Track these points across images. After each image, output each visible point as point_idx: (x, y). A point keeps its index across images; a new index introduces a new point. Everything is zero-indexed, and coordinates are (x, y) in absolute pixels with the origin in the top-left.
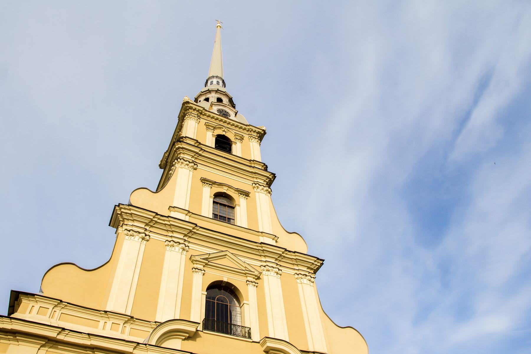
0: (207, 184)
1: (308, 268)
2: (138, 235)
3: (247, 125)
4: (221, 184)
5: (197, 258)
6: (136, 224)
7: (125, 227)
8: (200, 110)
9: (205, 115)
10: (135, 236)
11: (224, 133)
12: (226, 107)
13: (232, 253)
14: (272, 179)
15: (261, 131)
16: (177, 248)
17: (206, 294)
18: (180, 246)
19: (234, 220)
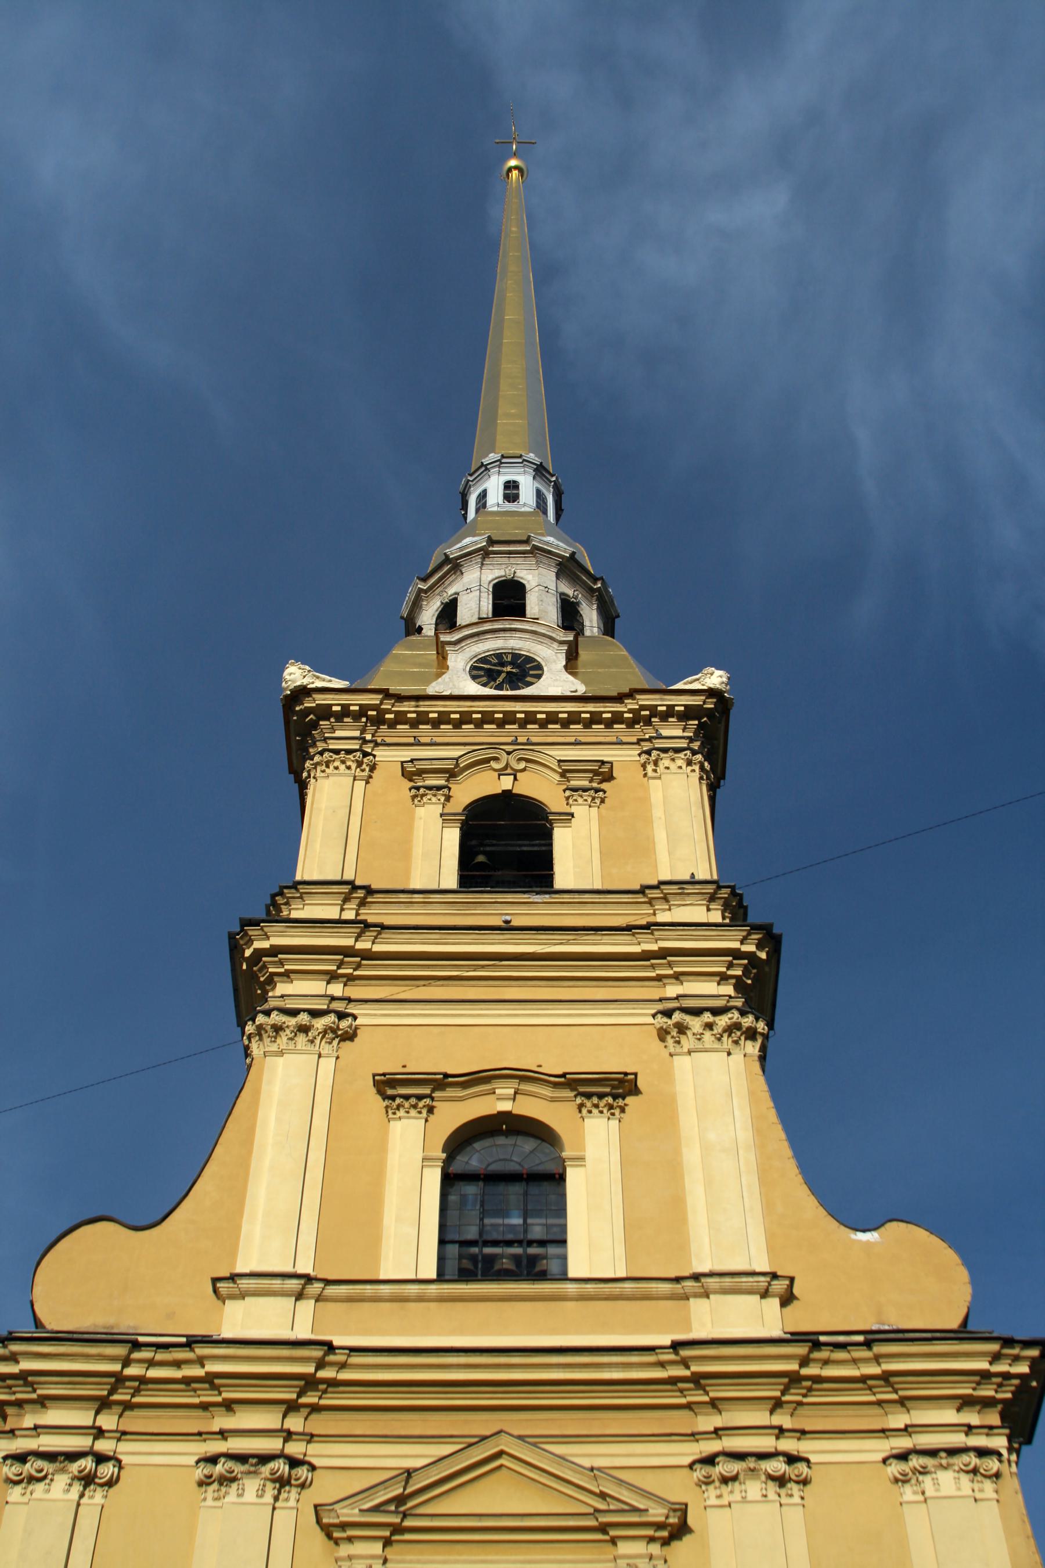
0: (407, 1097)
3: (619, 698)
11: (506, 783)
14: (763, 955)
16: (251, 1485)
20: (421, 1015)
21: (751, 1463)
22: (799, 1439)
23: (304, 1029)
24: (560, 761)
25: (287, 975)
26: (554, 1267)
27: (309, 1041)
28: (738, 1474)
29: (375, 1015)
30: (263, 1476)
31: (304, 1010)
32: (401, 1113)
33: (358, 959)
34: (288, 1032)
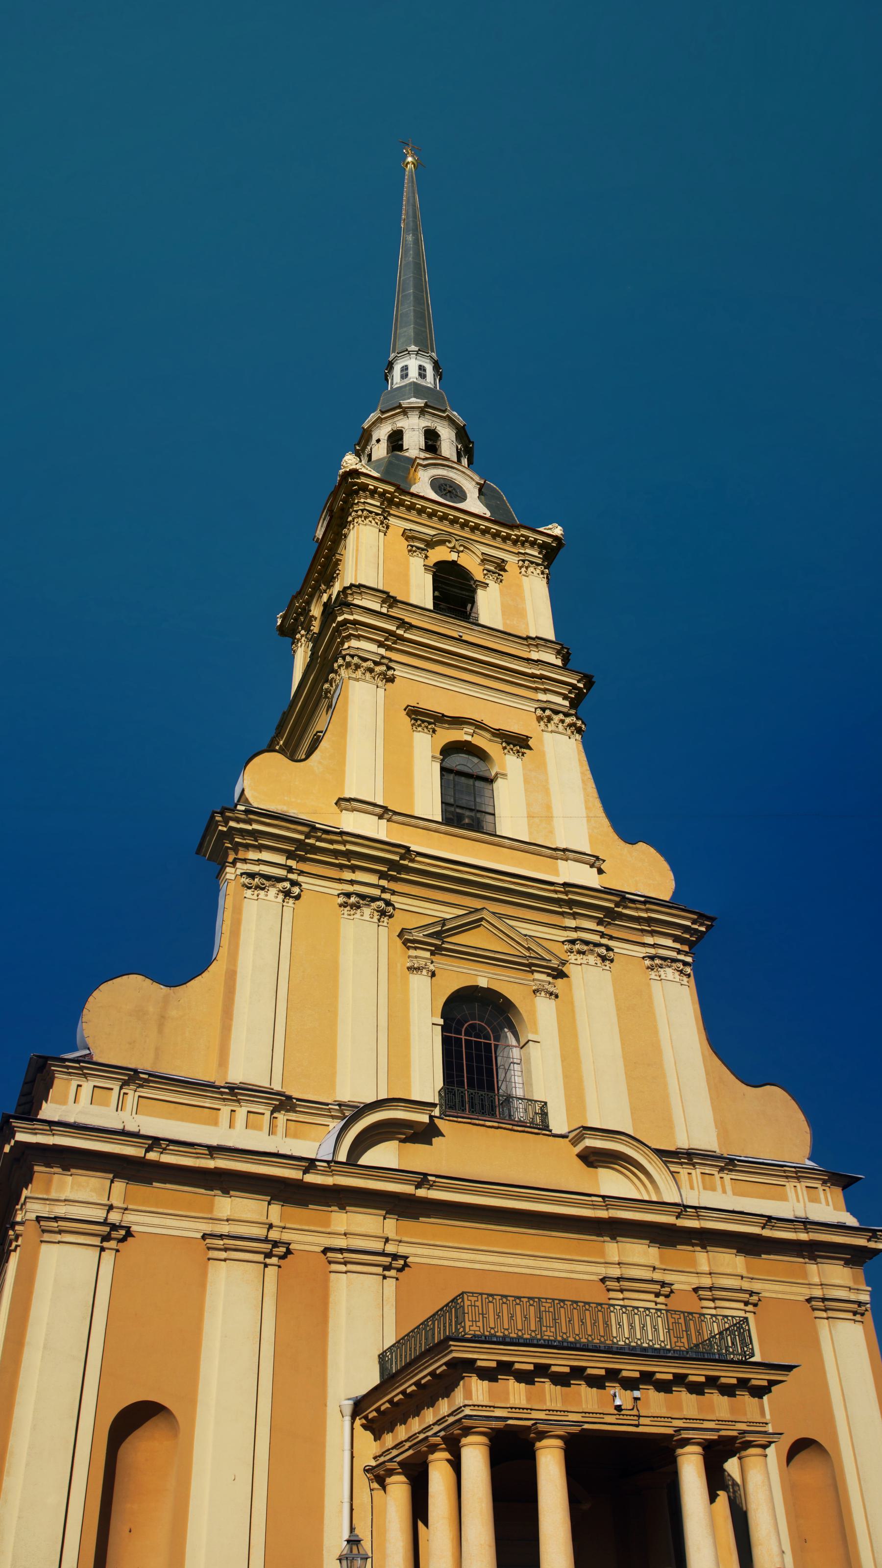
0: (423, 721)
1: (676, 939)
2: (273, 886)
4: (457, 722)
5: (416, 936)
6: (266, 856)
7: (242, 867)
8: (389, 492)
9: (401, 504)
10: (267, 888)
12: (454, 471)
13: (494, 913)
14: (585, 691)
15: (549, 540)
17: (443, 1024)
18: (372, 904)
19: (492, 817)
20: (426, 678)
21: (591, 947)
22: (609, 940)
23: (371, 670)
24: (483, 553)
25: (358, 637)
26: (488, 827)
27: (372, 677)
28: (585, 951)
29: (402, 671)
30: (372, 908)
31: (371, 660)
32: (420, 729)
33: (395, 639)
34: (362, 669)
